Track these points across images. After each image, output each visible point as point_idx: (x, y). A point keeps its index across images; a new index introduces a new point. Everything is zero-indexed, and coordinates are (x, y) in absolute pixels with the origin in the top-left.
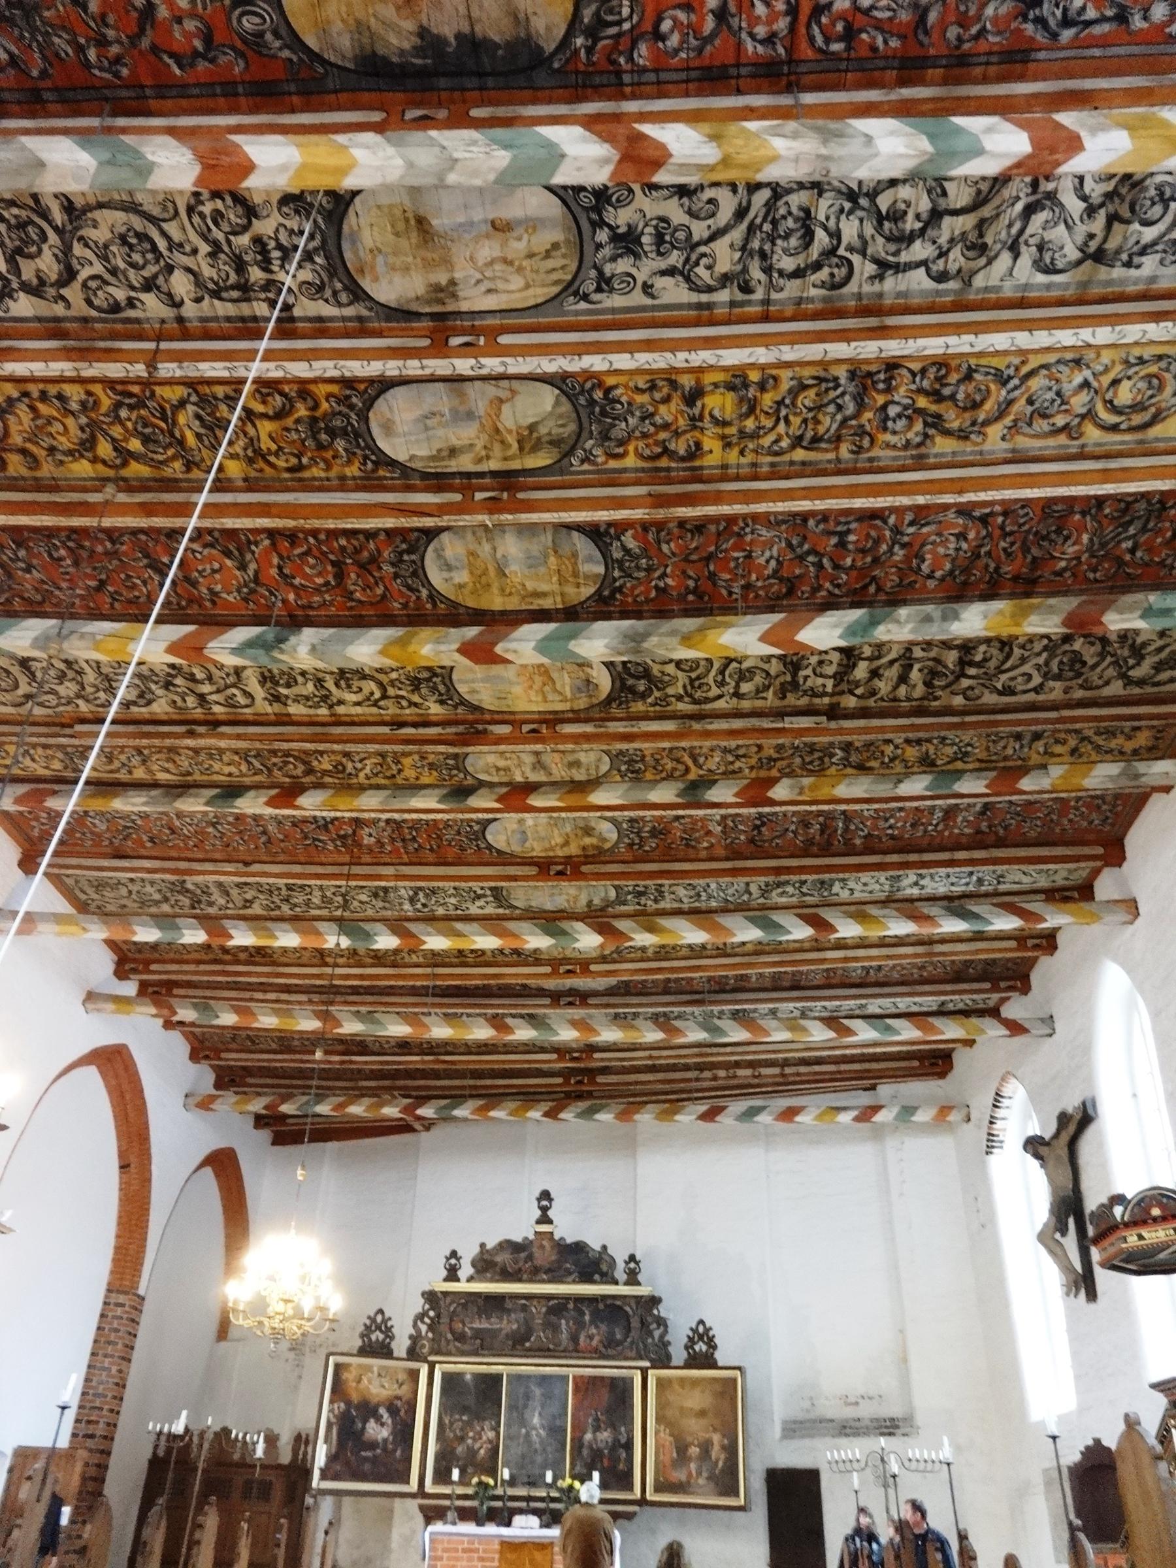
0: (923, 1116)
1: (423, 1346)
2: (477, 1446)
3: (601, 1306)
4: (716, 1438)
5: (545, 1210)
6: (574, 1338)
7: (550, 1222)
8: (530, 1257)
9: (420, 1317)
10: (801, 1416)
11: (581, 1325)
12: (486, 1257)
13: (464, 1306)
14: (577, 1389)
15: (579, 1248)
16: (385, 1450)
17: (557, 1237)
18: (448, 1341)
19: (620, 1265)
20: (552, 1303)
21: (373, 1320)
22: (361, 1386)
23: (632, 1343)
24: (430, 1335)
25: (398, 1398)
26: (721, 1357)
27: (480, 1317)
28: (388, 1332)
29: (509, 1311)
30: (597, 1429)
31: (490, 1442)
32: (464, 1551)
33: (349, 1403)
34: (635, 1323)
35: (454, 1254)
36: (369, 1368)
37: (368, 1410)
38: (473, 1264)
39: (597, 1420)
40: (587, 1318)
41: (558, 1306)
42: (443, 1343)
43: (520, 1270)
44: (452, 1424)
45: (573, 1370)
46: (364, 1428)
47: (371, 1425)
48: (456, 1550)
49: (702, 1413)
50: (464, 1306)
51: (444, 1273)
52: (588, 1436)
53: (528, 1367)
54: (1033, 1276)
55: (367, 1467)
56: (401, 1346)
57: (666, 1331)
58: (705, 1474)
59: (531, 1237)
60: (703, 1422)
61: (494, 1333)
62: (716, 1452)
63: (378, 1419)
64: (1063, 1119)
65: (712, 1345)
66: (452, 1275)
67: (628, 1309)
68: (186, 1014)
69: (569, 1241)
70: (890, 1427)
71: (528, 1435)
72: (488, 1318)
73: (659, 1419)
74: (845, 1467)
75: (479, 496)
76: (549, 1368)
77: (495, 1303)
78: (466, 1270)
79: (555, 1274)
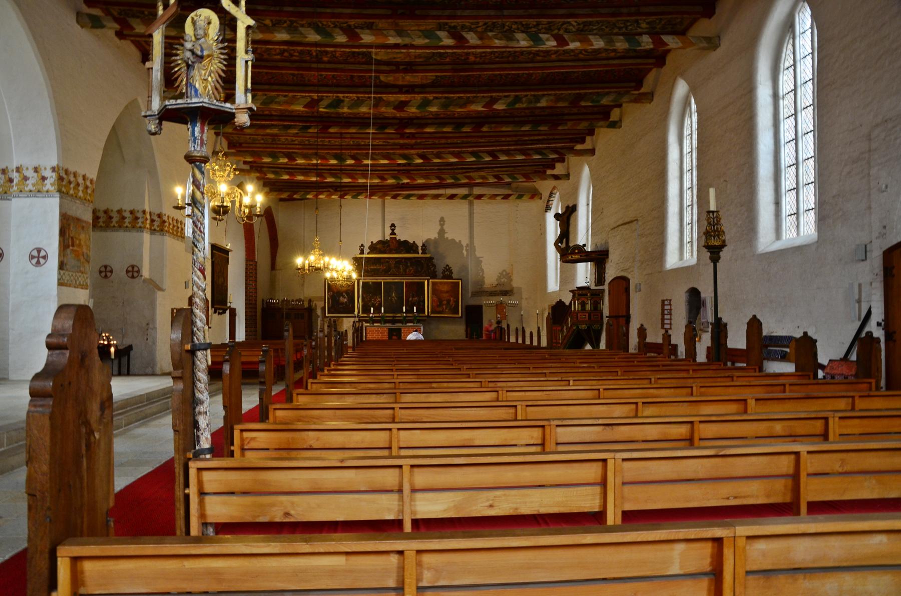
0: (524, 198)
5: (393, 230)
8: (389, 246)
15: (406, 242)
19: (420, 248)
26: (454, 276)
35: (362, 245)
45: (405, 280)
47: (341, 298)
49: (447, 292)
53: (390, 279)
54: (552, 255)
61: (378, 270)
64: (568, 207)
66: (362, 252)
68: (271, 176)
70: (505, 293)
73: (433, 294)
74: (490, 305)
75: (401, 67)
76: (397, 279)
78: (366, 250)
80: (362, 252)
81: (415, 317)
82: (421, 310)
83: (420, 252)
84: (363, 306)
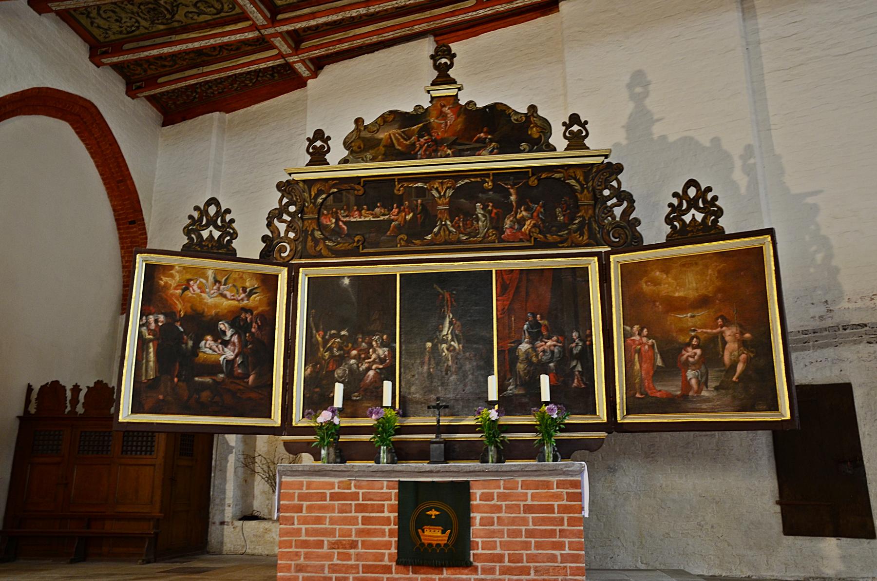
1: (283, 249)
2: (365, 366)
3: (533, 181)
4: (729, 333)
6: (497, 226)
7: (454, 82)
8: (427, 129)
9: (275, 215)
10: (816, 324)
11: (507, 208)
12: (364, 134)
13: (337, 197)
14: (503, 289)
16: (230, 373)
17: (462, 102)
18: (316, 241)
20: (461, 183)
21: (203, 212)
22: (189, 294)
23: (582, 225)
24: (291, 235)
25: (244, 309)
27: (360, 210)
28: (228, 230)
29: (400, 200)
30: (536, 336)
31: (382, 361)
32: (334, 497)
33: (171, 315)
34: (585, 198)
35: (319, 134)
36: (201, 272)
37: (203, 324)
38: (347, 144)
39: (535, 325)
40: (513, 198)
41: (469, 187)
42: (310, 243)
43: (414, 144)
44: (325, 342)
46: (196, 346)
47: (208, 345)
48: (323, 497)
49: (703, 302)
50: (337, 197)
51: (308, 158)
52: (524, 347)
55: (205, 395)
56: (248, 244)
57: (631, 208)
58: (712, 384)
59: (426, 104)
60: (702, 315)
61: (381, 227)
62: (731, 350)
63: (218, 336)
65: (713, 210)
66: (318, 157)
67: (572, 182)
69: (480, 104)
71: (435, 347)
72: (371, 208)
73: (627, 320)
77: (379, 191)
78: (337, 152)
79: (462, 145)
80: (318, 157)
81: (547, 427)
82: (575, 394)
83: (558, 140)
84: (308, 382)
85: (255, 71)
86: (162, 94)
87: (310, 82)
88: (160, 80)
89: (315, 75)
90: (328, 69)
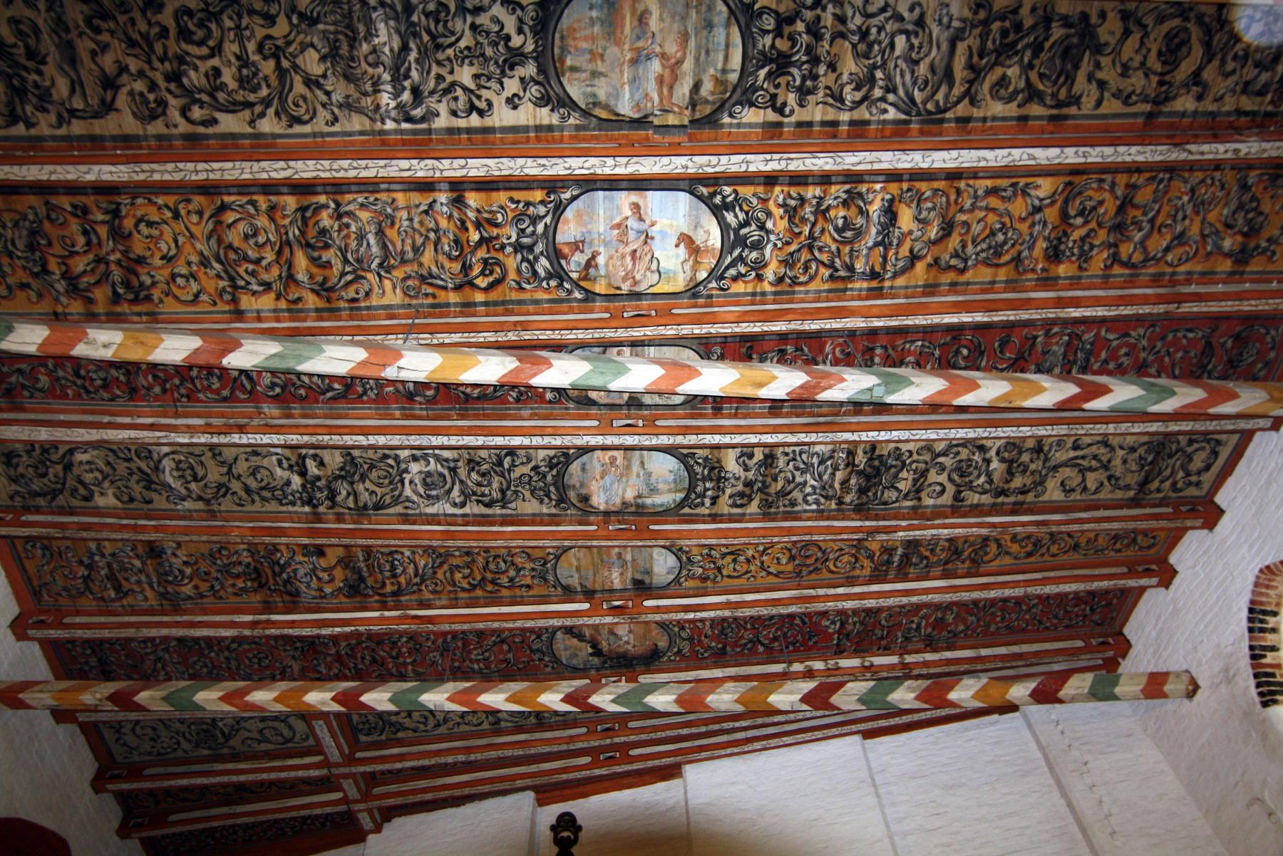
85: (303, 817)
86: (165, 837)
87: (371, 837)
88: (173, 818)
89: (378, 829)
90: (398, 822)
